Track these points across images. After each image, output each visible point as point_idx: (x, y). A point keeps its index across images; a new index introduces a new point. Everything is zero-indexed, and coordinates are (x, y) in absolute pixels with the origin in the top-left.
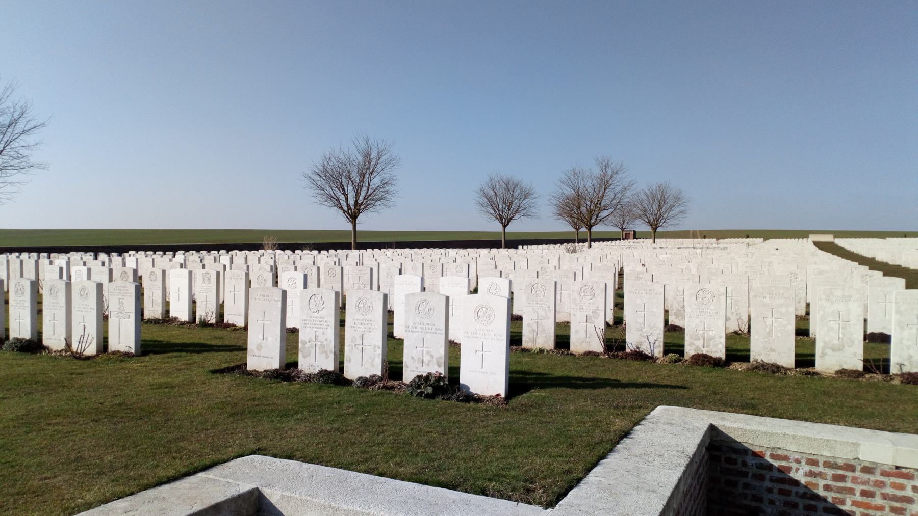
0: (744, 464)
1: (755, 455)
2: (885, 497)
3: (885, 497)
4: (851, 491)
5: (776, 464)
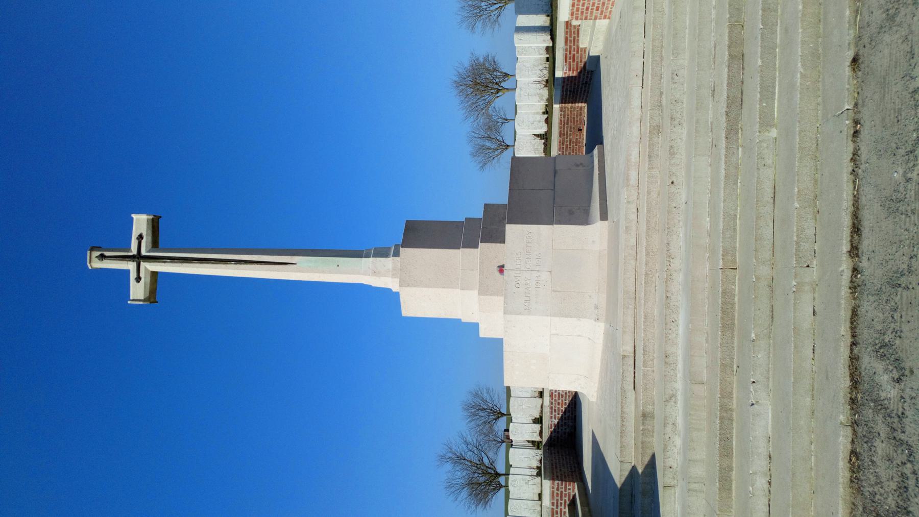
0: (555, 436)
1: (551, 433)
2: (559, 399)
3: (559, 399)
4: (558, 408)
5: (553, 428)
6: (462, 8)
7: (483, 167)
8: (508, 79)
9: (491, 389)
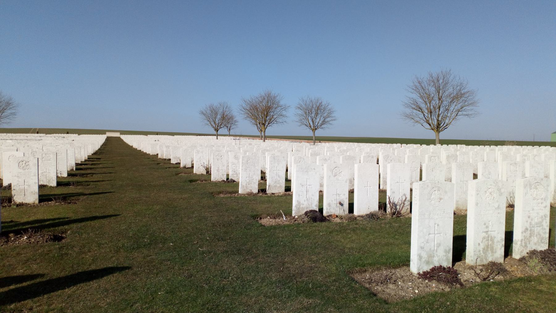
6: (311, 101)
7: (203, 113)
8: (259, 130)
9: (16, 116)
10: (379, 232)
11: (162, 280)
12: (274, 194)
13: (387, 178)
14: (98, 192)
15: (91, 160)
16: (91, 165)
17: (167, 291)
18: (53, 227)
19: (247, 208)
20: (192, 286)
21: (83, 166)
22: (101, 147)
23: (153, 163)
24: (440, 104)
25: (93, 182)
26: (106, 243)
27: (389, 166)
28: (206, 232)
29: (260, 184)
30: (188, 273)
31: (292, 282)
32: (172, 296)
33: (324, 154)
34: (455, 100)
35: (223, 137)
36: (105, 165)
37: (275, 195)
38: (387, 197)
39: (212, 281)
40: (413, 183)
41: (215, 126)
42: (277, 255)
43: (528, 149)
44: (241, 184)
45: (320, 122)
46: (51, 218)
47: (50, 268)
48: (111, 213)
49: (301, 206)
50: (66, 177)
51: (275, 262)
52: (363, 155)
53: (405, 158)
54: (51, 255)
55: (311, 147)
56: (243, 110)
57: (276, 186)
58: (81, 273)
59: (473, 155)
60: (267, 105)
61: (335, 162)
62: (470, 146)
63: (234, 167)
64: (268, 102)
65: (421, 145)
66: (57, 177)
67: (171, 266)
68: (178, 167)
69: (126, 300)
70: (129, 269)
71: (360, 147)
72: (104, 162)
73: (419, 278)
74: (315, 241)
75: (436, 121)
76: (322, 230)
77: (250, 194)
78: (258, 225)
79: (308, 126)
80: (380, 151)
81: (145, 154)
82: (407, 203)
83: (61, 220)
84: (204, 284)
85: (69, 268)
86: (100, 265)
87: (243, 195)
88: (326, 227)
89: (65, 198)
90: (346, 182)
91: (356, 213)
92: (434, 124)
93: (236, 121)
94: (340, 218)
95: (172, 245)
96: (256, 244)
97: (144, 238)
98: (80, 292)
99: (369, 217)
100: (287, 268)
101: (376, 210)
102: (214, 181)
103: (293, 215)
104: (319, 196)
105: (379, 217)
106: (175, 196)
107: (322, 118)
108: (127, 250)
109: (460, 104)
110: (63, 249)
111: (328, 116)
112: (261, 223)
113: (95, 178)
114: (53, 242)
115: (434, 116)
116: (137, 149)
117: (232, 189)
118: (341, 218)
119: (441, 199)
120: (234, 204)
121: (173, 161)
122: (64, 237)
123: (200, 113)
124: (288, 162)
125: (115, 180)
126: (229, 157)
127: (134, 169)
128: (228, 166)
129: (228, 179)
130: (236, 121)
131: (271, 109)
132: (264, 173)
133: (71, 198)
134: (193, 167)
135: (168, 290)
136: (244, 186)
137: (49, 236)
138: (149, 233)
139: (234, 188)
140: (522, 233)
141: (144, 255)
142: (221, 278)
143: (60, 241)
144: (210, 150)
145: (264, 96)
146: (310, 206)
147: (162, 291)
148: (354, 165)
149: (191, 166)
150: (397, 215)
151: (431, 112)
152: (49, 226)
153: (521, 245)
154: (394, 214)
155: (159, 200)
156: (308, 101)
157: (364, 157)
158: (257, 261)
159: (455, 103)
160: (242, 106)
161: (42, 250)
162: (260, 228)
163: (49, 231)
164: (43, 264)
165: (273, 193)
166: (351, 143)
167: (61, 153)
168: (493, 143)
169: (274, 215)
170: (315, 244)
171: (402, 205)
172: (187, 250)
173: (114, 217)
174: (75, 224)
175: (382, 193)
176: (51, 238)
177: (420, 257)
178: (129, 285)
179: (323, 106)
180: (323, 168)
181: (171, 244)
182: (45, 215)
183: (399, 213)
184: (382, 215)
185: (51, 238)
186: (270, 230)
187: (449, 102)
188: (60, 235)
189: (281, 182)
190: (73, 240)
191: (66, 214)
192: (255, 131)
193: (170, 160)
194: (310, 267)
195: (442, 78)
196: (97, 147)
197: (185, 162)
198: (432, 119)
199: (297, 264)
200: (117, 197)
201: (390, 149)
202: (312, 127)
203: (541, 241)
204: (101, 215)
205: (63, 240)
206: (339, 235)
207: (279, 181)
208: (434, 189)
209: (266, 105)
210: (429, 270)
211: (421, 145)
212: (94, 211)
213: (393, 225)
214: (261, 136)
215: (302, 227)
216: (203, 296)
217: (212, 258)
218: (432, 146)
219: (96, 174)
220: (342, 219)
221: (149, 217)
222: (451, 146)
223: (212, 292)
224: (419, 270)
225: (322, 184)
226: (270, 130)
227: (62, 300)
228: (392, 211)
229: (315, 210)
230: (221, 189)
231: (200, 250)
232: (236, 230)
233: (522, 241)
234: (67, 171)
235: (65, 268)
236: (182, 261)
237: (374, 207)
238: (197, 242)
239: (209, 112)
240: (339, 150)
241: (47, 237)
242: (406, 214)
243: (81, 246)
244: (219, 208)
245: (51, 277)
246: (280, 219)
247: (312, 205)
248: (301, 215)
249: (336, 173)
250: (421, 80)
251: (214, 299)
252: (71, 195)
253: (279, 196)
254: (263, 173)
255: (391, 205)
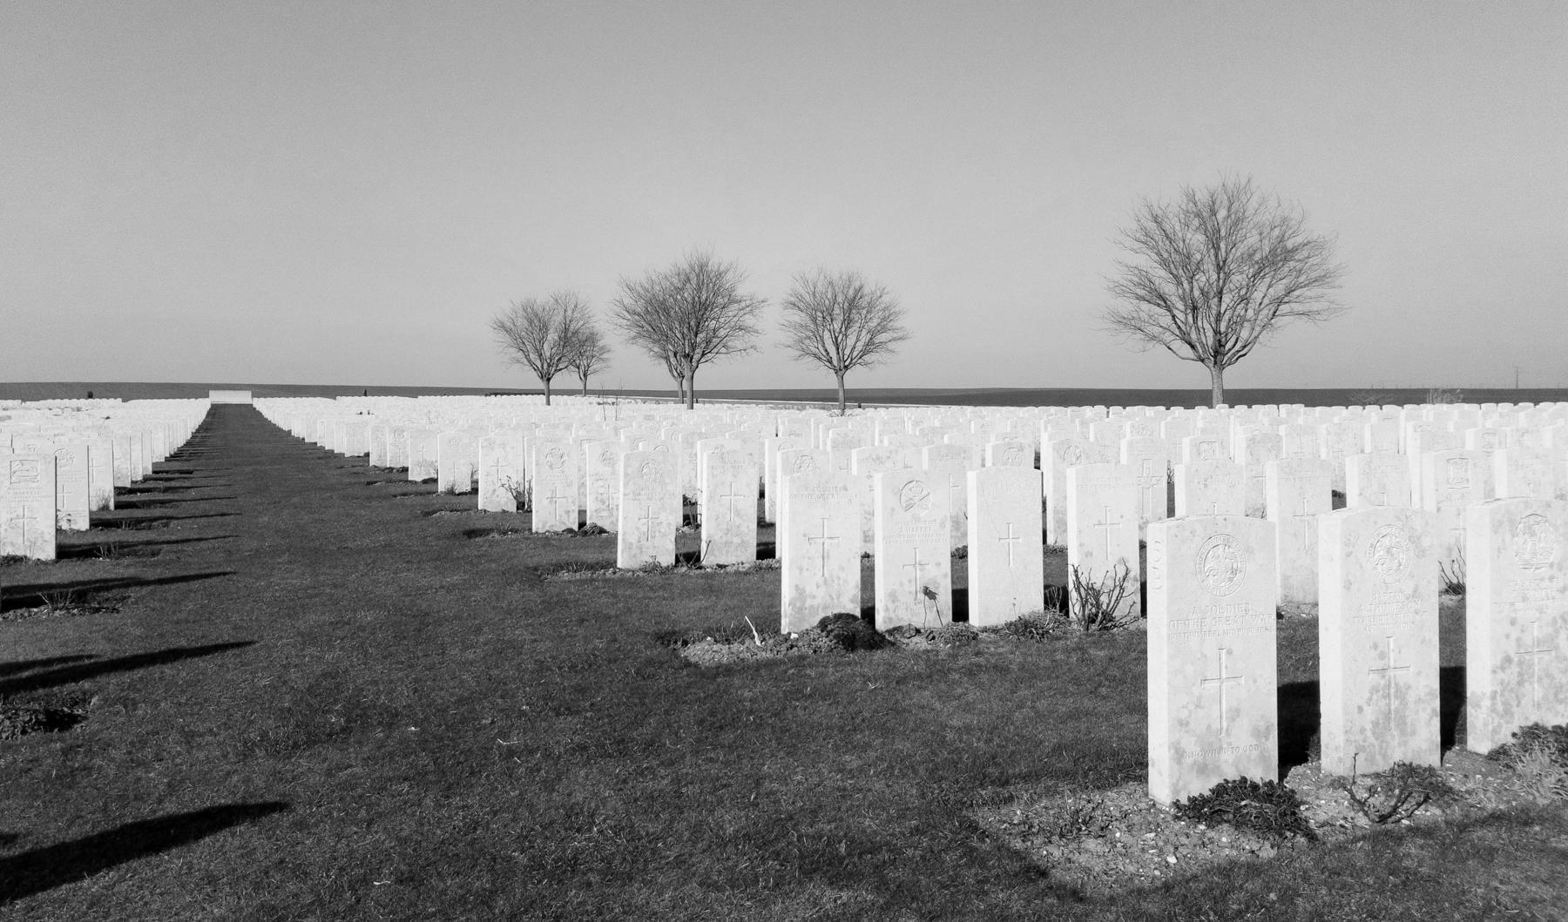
6: (831, 283)
7: (503, 326)
10: (1049, 678)
11: (383, 843)
12: (725, 566)
13: (1066, 510)
14: (185, 573)
15: (164, 475)
16: (164, 492)
17: (399, 874)
18: (44, 686)
19: (642, 613)
20: (478, 859)
21: (139, 497)
22: (193, 437)
23: (353, 481)
24: (1221, 281)
25: (168, 542)
26: (211, 730)
27: (1071, 473)
28: (518, 688)
29: (680, 538)
30: (464, 818)
31: (784, 837)
32: (415, 890)
33: (873, 441)
34: (1267, 270)
35: (565, 397)
36: (207, 492)
37: (728, 569)
38: (1071, 569)
39: (538, 841)
40: (1146, 523)
41: (543, 368)
42: (738, 756)
43: (1500, 413)
44: (623, 540)
45: (860, 346)
46: (40, 658)
47: (35, 816)
48: (226, 638)
49: (809, 602)
50: (87, 530)
51: (732, 777)
52: (993, 441)
53: (1119, 449)
54: (37, 773)
55: (833, 421)
56: (626, 314)
57: (732, 543)
58: (132, 826)
59: (1329, 434)
60: (697, 299)
61: (906, 467)
62: (1318, 409)
63: (602, 486)
64: (699, 289)
65: (1168, 409)
66: (59, 531)
67: (411, 796)
68: (429, 493)
69: (273, 908)
70: (281, 810)
71: (983, 418)
72: (204, 482)
73: (1177, 818)
74: (852, 709)
75: (1210, 333)
76: (874, 675)
77: (653, 569)
78: (676, 663)
79: (823, 357)
80: (1042, 427)
81: (330, 456)
82: (1132, 587)
83: (71, 664)
84: (514, 851)
85: (94, 813)
86: (192, 800)
87: (631, 573)
88: (885, 664)
89: (82, 596)
90: (943, 525)
91: (976, 619)
92: (1204, 342)
93: (603, 350)
94: (927, 637)
95: (415, 733)
96: (672, 720)
97: (328, 712)
98: (129, 886)
99: (1016, 632)
100: (768, 795)
101: (1036, 610)
102: (540, 531)
103: (784, 631)
104: (862, 571)
105: (1047, 632)
106: (424, 582)
107: (864, 332)
108: (276, 750)
109: (1284, 281)
110: (77, 753)
111: (882, 328)
112: (686, 657)
113: (177, 530)
114: (46, 731)
115: (1205, 321)
116: (304, 439)
117: (596, 556)
118: (931, 636)
119: (1234, 572)
120: (604, 600)
121: (416, 475)
122: (79, 715)
123: (495, 326)
124: (764, 468)
125: (236, 536)
126: (585, 459)
127: (295, 500)
128: (583, 485)
129: (582, 525)
130: (603, 350)
131: (709, 309)
132: (694, 504)
133: (102, 594)
134: (475, 491)
135: (402, 874)
136: (632, 544)
137: (31, 715)
138: (343, 695)
139: (601, 553)
140: (1494, 672)
141: (329, 765)
142: (566, 829)
143: (67, 730)
144: (525, 439)
145: (688, 271)
146: (835, 601)
147: (385, 876)
148: (965, 473)
149: (469, 489)
150: (1101, 622)
151: (1195, 309)
152: (31, 684)
153: (1493, 710)
154: (1092, 620)
155: (372, 596)
156: (819, 284)
157: (995, 448)
158: (677, 776)
159: (1267, 280)
160: (621, 302)
161: (10, 758)
162: (685, 673)
163: (33, 699)
164: (11, 802)
165: (721, 563)
166: (955, 408)
167: (68, 457)
168: (1390, 397)
169: (725, 631)
170: (853, 718)
171: (1116, 592)
172: (462, 746)
173: (236, 651)
174: (112, 675)
175: (1055, 556)
176: (38, 722)
177: (1179, 754)
178: (282, 861)
179: (867, 299)
180: (870, 487)
181: (413, 728)
182: (19, 650)
183: (1107, 618)
184: (1056, 625)
185: (38, 722)
186: (715, 678)
187: (1250, 276)
188: (66, 709)
189: (746, 530)
190: (108, 725)
191: (84, 645)
192: (660, 375)
193: (405, 470)
194: (839, 789)
195: (1226, 203)
196: (181, 437)
197: (451, 477)
198: (1197, 328)
199: (799, 783)
200: (245, 586)
201: (1073, 421)
202: (835, 363)
203: (1556, 695)
204: (193, 643)
205: (76, 726)
206: (926, 688)
207: (738, 527)
208: (1213, 542)
209: (694, 298)
210: (1207, 793)
211: (1168, 409)
212: (173, 633)
213: (1090, 655)
214: (680, 394)
215: (811, 666)
216: (514, 889)
217: (539, 770)
218: (1201, 412)
219: (177, 518)
220: (934, 638)
221: (342, 649)
222: (1260, 410)
223: (538, 874)
224: (1176, 791)
225: (870, 533)
226: (708, 375)
227: (73, 916)
228: (1087, 612)
229: (852, 613)
230: (564, 556)
231: (500, 746)
232: (609, 681)
233: (1493, 697)
234: (87, 514)
235: (83, 813)
236: (446, 781)
237: (1032, 602)
238: (490, 719)
239: (522, 323)
240: (917, 429)
241: (27, 719)
242: (1128, 618)
243: (132, 743)
244: (558, 613)
245: (37, 843)
246: (743, 643)
247: (841, 599)
248: (807, 630)
249: (911, 499)
250: (1160, 213)
251: (545, 896)
252: (102, 584)
253: (740, 573)
254: (689, 503)
255: (1083, 594)
